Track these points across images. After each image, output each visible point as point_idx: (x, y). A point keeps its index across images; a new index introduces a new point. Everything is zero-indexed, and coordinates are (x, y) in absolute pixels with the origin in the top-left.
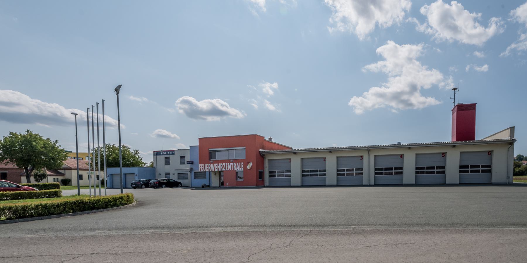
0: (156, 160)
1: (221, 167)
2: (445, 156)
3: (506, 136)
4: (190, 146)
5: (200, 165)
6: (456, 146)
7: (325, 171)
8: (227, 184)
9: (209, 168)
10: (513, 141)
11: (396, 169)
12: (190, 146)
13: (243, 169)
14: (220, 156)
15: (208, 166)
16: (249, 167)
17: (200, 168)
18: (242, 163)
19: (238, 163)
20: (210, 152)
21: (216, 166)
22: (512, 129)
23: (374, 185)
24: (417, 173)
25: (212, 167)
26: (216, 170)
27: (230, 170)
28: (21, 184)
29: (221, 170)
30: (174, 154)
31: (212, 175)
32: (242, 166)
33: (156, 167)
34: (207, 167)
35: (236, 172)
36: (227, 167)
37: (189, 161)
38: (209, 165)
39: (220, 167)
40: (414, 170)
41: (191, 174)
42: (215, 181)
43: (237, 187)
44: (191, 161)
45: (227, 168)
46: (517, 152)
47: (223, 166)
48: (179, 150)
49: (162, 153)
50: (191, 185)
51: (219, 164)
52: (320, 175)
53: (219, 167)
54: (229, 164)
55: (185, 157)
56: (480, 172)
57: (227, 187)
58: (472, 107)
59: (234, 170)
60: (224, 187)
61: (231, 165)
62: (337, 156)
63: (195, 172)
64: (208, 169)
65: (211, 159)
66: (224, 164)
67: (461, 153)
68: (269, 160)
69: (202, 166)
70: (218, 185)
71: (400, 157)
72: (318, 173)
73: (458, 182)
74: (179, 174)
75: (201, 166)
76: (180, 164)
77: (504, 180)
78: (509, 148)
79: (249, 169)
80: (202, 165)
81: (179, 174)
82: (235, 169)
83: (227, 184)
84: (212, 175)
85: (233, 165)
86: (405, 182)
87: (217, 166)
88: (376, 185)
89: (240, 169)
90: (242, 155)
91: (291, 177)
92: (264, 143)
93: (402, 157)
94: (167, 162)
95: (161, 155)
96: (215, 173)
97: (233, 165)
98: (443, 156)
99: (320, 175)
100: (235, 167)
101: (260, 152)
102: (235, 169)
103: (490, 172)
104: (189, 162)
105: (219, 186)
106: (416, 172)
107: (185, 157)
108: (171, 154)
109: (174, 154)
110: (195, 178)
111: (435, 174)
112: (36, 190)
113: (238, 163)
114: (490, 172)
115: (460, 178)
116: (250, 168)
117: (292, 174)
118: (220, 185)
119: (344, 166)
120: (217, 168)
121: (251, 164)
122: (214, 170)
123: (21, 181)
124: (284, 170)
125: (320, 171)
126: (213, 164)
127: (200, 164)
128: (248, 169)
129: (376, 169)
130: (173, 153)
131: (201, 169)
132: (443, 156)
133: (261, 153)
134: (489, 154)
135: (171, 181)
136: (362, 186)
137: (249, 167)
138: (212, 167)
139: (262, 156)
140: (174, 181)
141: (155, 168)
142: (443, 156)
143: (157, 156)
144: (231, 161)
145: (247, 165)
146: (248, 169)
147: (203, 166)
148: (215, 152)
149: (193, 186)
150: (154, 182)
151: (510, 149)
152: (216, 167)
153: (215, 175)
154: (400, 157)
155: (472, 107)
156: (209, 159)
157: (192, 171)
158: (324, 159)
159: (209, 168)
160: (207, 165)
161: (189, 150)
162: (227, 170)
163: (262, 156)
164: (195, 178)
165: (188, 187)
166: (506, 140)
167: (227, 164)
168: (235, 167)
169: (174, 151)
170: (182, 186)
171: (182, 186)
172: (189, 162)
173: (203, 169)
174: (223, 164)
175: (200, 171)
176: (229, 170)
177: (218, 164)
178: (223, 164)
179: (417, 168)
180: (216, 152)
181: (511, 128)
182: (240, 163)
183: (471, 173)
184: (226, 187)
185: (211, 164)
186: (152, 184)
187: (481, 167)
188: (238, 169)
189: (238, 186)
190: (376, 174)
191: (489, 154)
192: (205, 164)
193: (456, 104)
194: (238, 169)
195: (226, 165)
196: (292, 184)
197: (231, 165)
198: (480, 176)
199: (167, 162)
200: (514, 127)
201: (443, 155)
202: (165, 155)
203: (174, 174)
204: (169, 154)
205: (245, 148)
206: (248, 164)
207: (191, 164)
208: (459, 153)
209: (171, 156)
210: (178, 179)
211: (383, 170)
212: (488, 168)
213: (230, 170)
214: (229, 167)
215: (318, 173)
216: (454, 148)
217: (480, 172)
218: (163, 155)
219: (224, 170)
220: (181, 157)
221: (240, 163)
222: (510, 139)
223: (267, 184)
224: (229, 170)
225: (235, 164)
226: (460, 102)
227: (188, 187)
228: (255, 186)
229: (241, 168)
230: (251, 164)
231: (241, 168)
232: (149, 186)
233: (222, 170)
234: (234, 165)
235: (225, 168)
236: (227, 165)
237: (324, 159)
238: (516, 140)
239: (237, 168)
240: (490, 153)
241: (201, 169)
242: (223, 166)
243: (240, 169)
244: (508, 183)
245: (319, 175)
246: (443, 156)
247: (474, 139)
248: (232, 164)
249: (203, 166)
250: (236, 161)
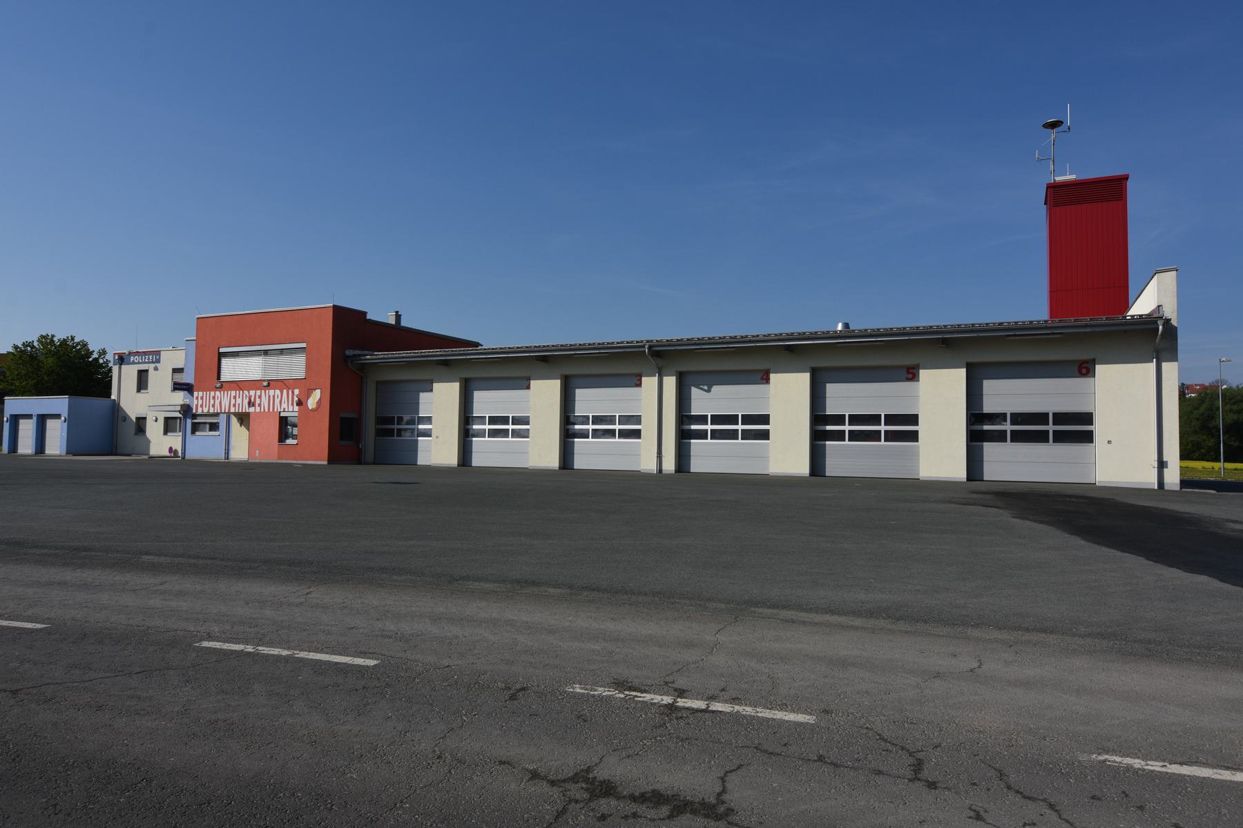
9: (217, 402)
15: (214, 398)
16: (312, 403)
19: (285, 391)
27: (266, 410)
59: (276, 410)
61: (269, 396)
64: (213, 406)
66: (252, 393)
68: (378, 383)
69: (199, 398)
79: (313, 410)
80: (201, 393)
85: (274, 396)
87: (235, 398)
97: (274, 396)
100: (277, 401)
104: (177, 386)
113: (285, 391)
116: (314, 406)
120: (234, 405)
121: (317, 394)
130: (158, 357)
131: (197, 406)
147: (202, 398)
159: (217, 402)
160: (212, 393)
168: (277, 401)
172: (177, 386)
173: (202, 406)
174: (249, 393)
176: (262, 410)
178: (249, 393)
197: (269, 396)
202: (139, 363)
205: (304, 345)
213: (266, 410)
214: (265, 401)
218: (134, 363)
223: (369, 454)
225: (278, 392)
229: (293, 405)
230: (317, 394)
231: (293, 405)
233: (247, 411)
234: (276, 396)
236: (260, 397)
248: (272, 392)
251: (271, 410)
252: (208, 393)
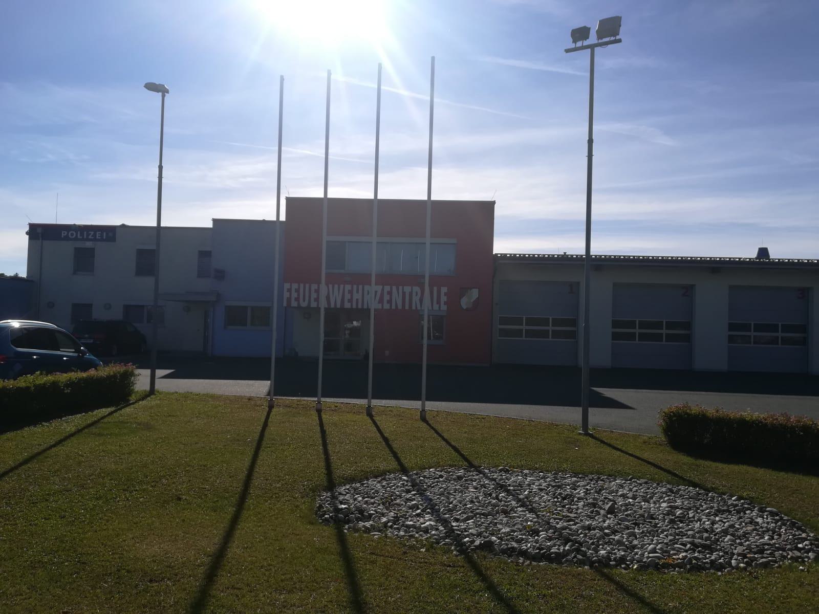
13: (444, 307)
18: (444, 290)
26: (347, 305)
27: (400, 307)
32: (444, 299)
34: (314, 295)
36: (386, 297)
45: (390, 302)
54: (394, 288)
59: (414, 308)
61: (404, 293)
69: (293, 291)
75: (289, 290)
79: (467, 309)
80: (295, 286)
85: (411, 294)
87: (351, 292)
97: (411, 294)
120: (350, 301)
126: (336, 286)
128: (465, 307)
146: (465, 307)
147: (297, 291)
152: (347, 296)
162: (387, 306)
168: (416, 299)
173: (297, 299)
176: (394, 307)
195: (385, 293)
197: (404, 293)
213: (400, 307)
229: (439, 302)
236: (390, 293)
241: (289, 300)
243: (436, 307)
249: (297, 291)
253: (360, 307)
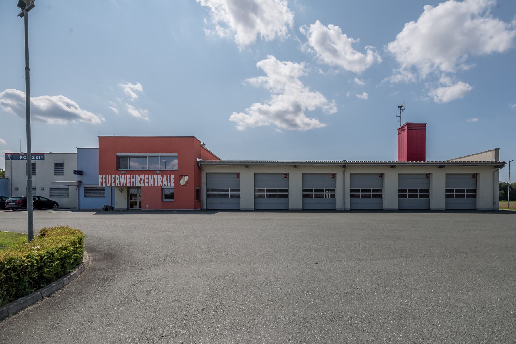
0: (10, 167)
1: (138, 181)
2: (476, 176)
3: (490, 158)
4: (77, 148)
5: (100, 176)
6: (396, 167)
7: (239, 190)
8: (148, 206)
9: (117, 181)
10: (503, 164)
11: (374, 190)
12: (77, 148)
13: (173, 185)
14: (133, 164)
15: (114, 179)
16: (183, 182)
17: (100, 181)
18: (172, 177)
19: (165, 177)
20: (118, 158)
21: (128, 179)
22: (497, 151)
23: (397, 209)
24: (304, 196)
25: (122, 180)
26: (128, 185)
27: (153, 185)
28: (1, 297)
29: (137, 185)
30: (43, 159)
31: (117, 192)
32: (172, 181)
33: (10, 178)
34: (113, 181)
35: (162, 189)
36: (146, 181)
37: (76, 169)
38: (117, 176)
39: (135, 181)
40: (301, 193)
41: (79, 190)
42: (121, 201)
43: (162, 210)
44: (79, 170)
45: (148, 183)
46: (503, 177)
47: (141, 179)
48: (50, 153)
49: (21, 157)
50: (79, 207)
51: (110, 176)
52: (231, 196)
53: (132, 180)
54: (107, 176)
55: (63, 164)
56: (464, 197)
57: (148, 210)
58: (422, 127)
59: (159, 185)
60: (142, 210)
61: (154, 179)
62: (255, 172)
63: (85, 187)
64: (114, 182)
65: (119, 168)
66: (142, 177)
67: (447, 174)
68: (207, 173)
69: (103, 179)
70: (126, 207)
71: (379, 177)
72: (277, 193)
73: (396, 207)
74: (51, 189)
75: (102, 179)
76: (54, 174)
77: (490, 206)
78: (495, 171)
79: (183, 185)
80: (104, 176)
81: (51, 189)
82: (161, 185)
83: (148, 206)
84: (117, 192)
85: (157, 179)
86: (385, 207)
87: (130, 179)
88: (352, 210)
89: (169, 184)
90: (174, 164)
91: (241, 198)
92: (200, 152)
93: (381, 177)
94: (31, 170)
95: (19, 159)
96: (121, 189)
97: (157, 179)
98: (426, 178)
99: (231, 196)
101: (198, 161)
102: (161, 185)
103: (429, 197)
104: (76, 172)
105: (128, 209)
106: (303, 194)
107: (63, 164)
108: (38, 159)
109: (43, 159)
110: (86, 195)
111: (372, 198)
112: (5, 293)
113: (165, 177)
114: (429, 197)
115: (447, 203)
116: (185, 184)
117: (290, 193)
118: (129, 207)
119: (314, 184)
120: (130, 183)
121: (186, 178)
122: (124, 185)
123: (446, 190)
124: (229, 189)
125: (232, 190)
126: (123, 176)
127: (100, 174)
128: (182, 184)
129: (352, 190)
131: (102, 183)
132: (426, 178)
133: (199, 163)
134: (474, 177)
135: (42, 199)
136: (334, 210)
137: (183, 182)
138: (122, 180)
139: (199, 167)
140: (46, 200)
141: (8, 179)
142: (427, 177)
143: (12, 161)
144: (158, 172)
145: (180, 179)
146: (182, 184)
147: (105, 179)
148: (127, 158)
149: (81, 208)
150: (14, 201)
151: (496, 173)
152: (128, 181)
153: (121, 192)
154: (379, 177)
155: (422, 127)
156: (117, 169)
157: (81, 185)
158: (285, 175)
159: (117, 181)
160: (113, 176)
161: (76, 154)
162: (147, 185)
163: (199, 167)
164: (86, 195)
165: (69, 208)
166: (492, 163)
167: (146, 177)
168: (160, 181)
169: (43, 154)
170: (59, 207)
171: (59, 207)
172: (76, 172)
173: (105, 182)
174: (140, 177)
175: (100, 185)
176: (150, 185)
177: (132, 176)
178: (140, 177)
179: (304, 190)
180: (128, 159)
181: (496, 149)
182: (168, 176)
183: (456, 198)
184: (146, 210)
185: (120, 176)
186: (10, 204)
187: (455, 191)
188: (165, 185)
189: (165, 210)
190: (352, 196)
191: (473, 178)
192: (110, 176)
193: (404, 122)
194: (165, 185)
195: (146, 179)
196: (242, 208)
197: (154, 179)
198: (419, 202)
199: (31, 170)
200: (499, 149)
201: (426, 176)
203: (43, 189)
204: (35, 159)
205: (176, 154)
206: (181, 177)
207: (79, 175)
208: (445, 174)
209: (38, 163)
210: (51, 196)
211: (407, 192)
212: (473, 193)
213: (153, 185)
214: (151, 181)
215: (419, 193)
216: (391, 168)
217: (464, 197)
219: (142, 185)
220: (56, 165)
221: (168, 176)
222: (495, 162)
223: (205, 207)
224: (150, 185)
225: (160, 176)
226: (410, 121)
227: (69, 208)
228: (192, 210)
229: (170, 182)
230: (186, 178)
231: (170, 182)
232: (4, 206)
233: (139, 185)
235: (144, 182)
236: (148, 179)
237: (285, 175)
238: (506, 163)
239: (164, 183)
240: (475, 176)
241: (102, 183)
242: (141, 179)
243: (169, 184)
244: (494, 210)
245: (230, 196)
246: (427, 177)
247: (424, 160)
248: (156, 177)
249: (130, 179)
250: (163, 173)
251: (156, 185)
252: (110, 176)
253: (137, 185)
